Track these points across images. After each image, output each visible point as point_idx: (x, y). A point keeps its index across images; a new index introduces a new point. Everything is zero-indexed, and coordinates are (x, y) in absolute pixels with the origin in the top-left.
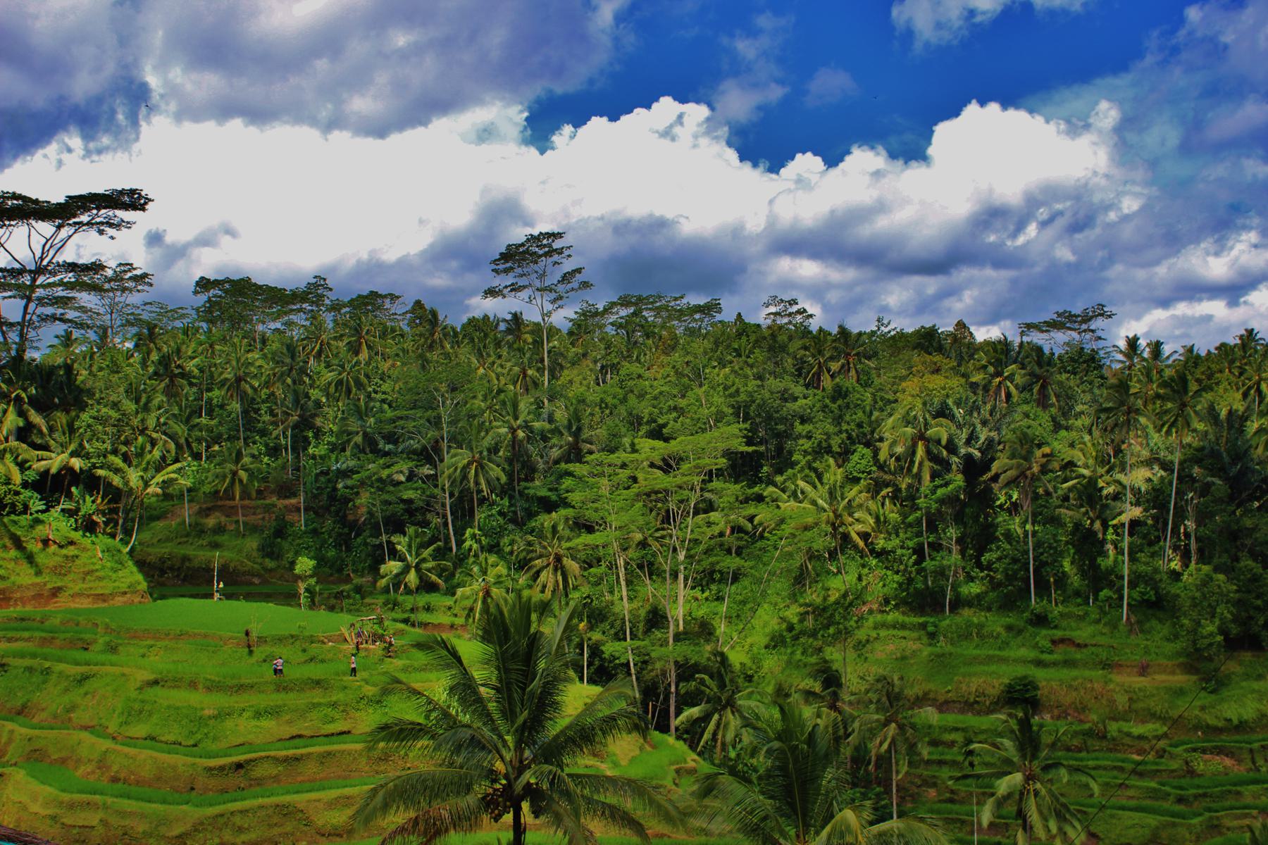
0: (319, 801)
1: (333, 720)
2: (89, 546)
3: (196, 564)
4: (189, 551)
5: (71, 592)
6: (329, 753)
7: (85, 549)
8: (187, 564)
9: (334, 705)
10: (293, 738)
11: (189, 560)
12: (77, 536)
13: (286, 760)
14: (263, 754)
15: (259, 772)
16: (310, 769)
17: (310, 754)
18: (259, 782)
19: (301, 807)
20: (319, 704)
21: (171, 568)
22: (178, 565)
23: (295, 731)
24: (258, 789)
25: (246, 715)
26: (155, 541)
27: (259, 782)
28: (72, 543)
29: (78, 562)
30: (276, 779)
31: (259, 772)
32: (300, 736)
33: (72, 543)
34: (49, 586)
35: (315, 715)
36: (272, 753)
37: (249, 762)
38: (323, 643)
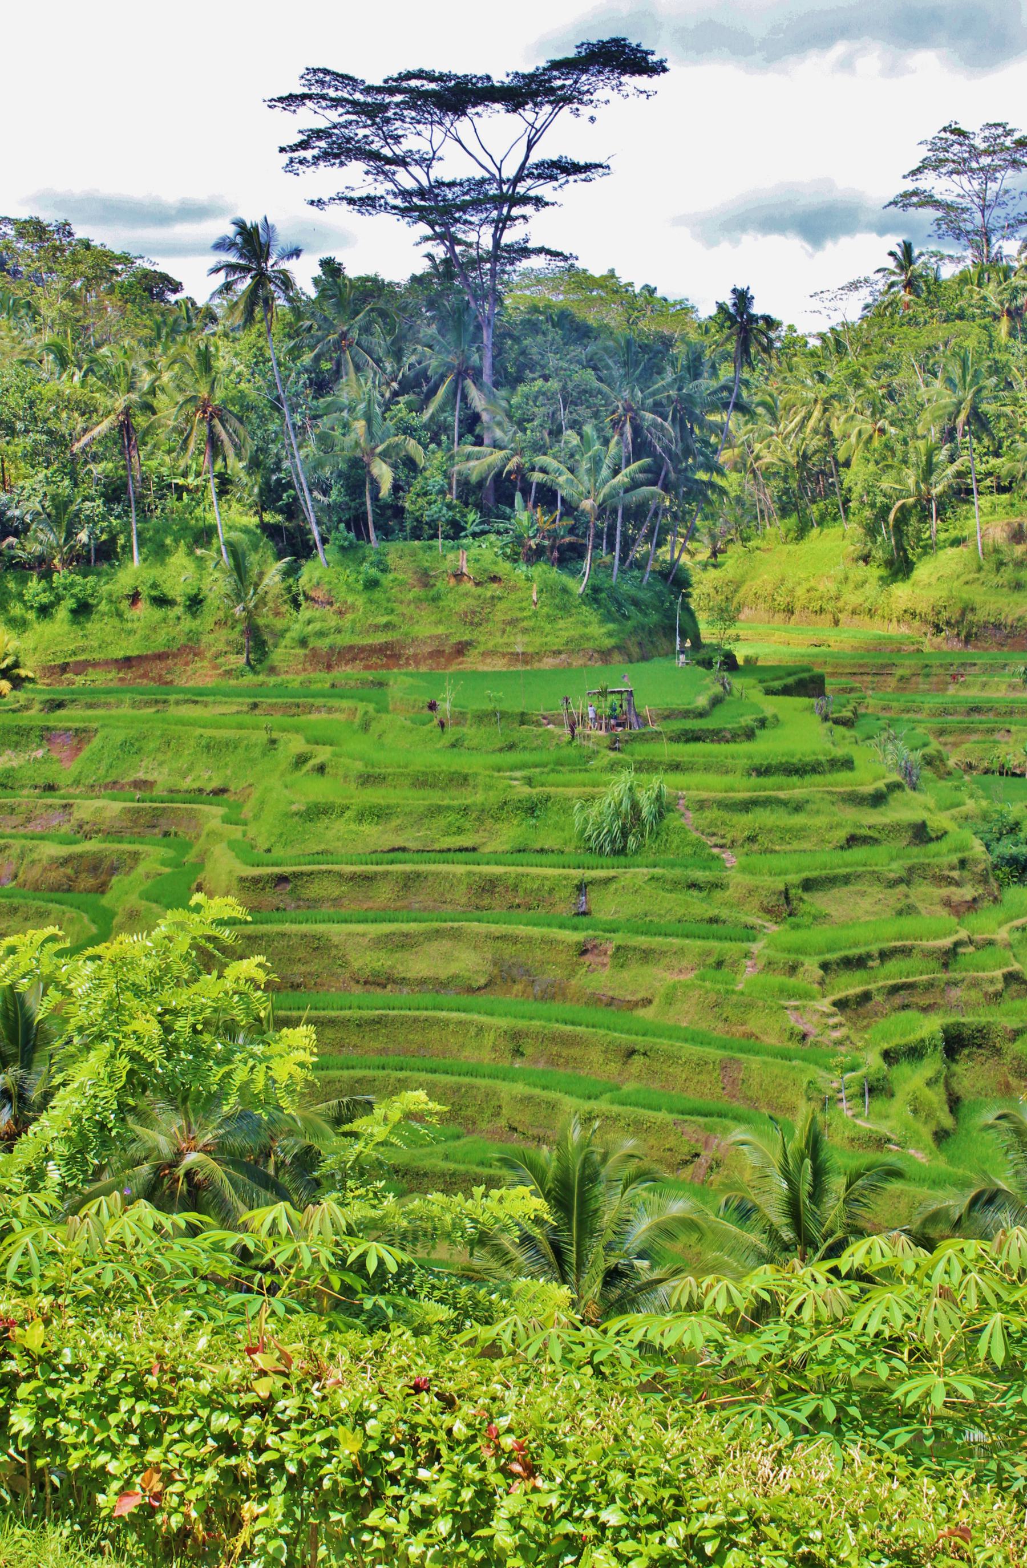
0: (364, 935)
1: (460, 831)
2: (522, 584)
3: (981, 616)
4: (977, 595)
5: (481, 648)
6: (418, 875)
7: (514, 588)
8: (970, 617)
9: (465, 810)
10: (393, 850)
11: (973, 610)
12: (504, 567)
13: (353, 877)
14: (324, 867)
15: (314, 890)
16: (384, 893)
17: (387, 873)
18: (313, 903)
19: (336, 940)
20: (448, 808)
21: (948, 623)
22: (955, 617)
23: (399, 842)
24: (302, 913)
25: (348, 814)
26: (933, 580)
27: (313, 903)
28: (495, 579)
29: (501, 606)
30: (336, 902)
31: (314, 890)
32: (403, 849)
33: (495, 579)
34: (453, 640)
35: (441, 822)
36: (336, 868)
37: (297, 875)
38: (538, 724)
